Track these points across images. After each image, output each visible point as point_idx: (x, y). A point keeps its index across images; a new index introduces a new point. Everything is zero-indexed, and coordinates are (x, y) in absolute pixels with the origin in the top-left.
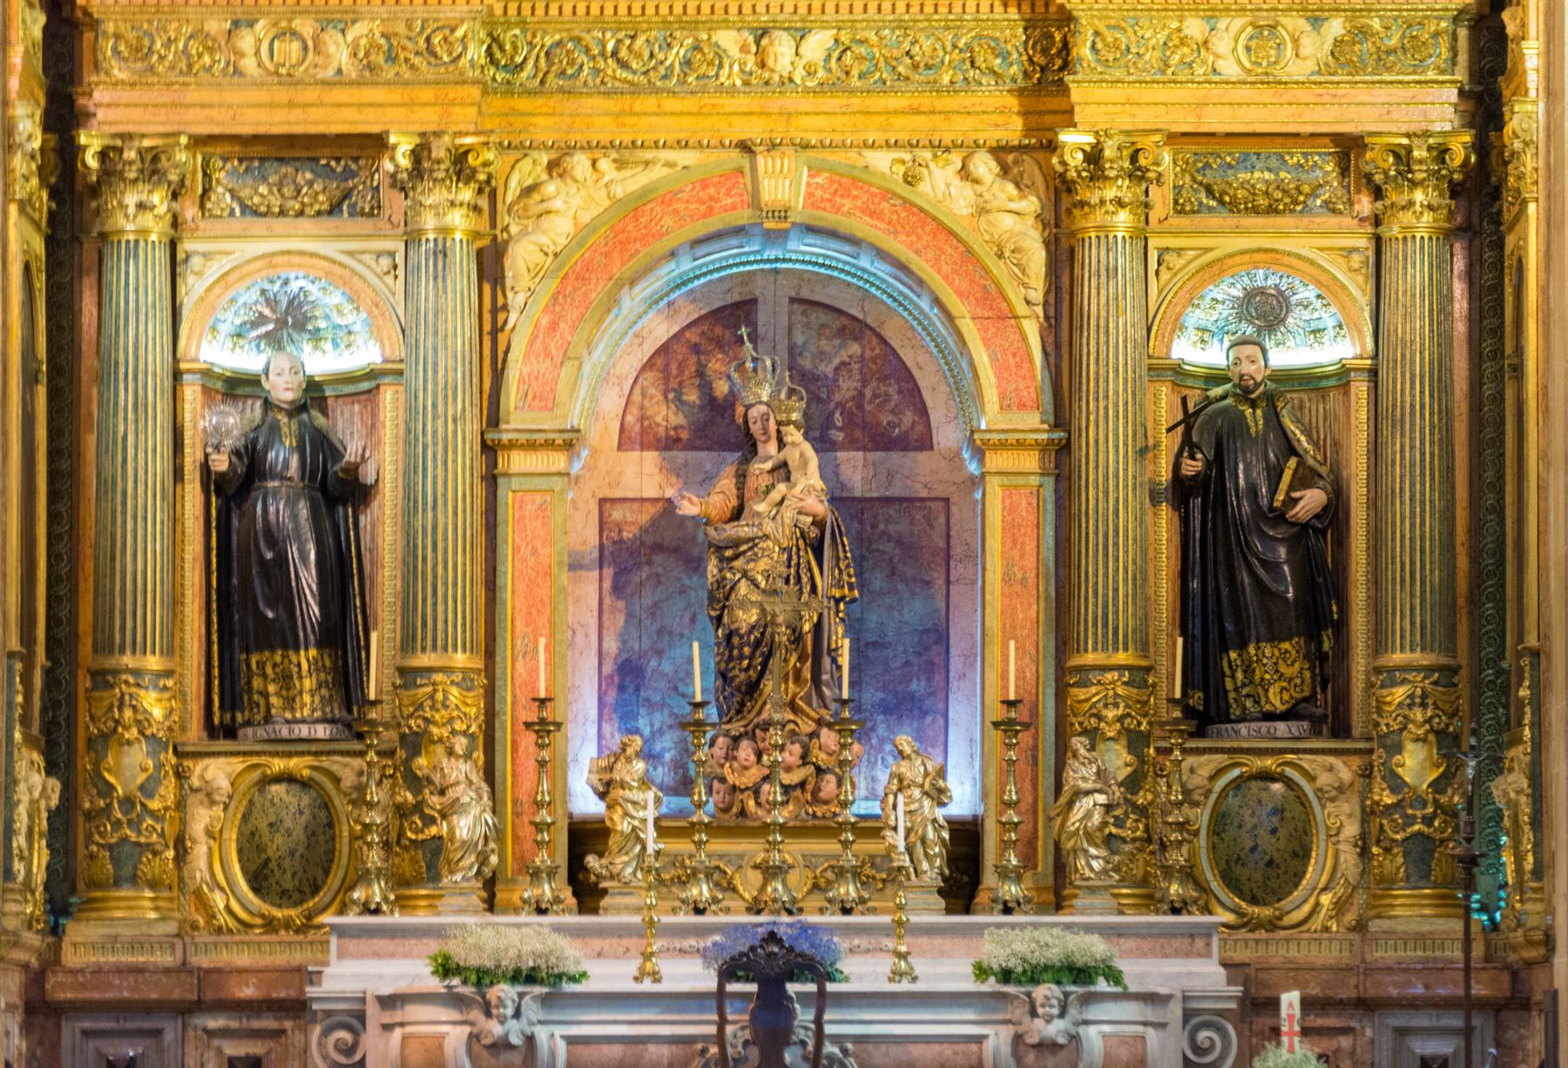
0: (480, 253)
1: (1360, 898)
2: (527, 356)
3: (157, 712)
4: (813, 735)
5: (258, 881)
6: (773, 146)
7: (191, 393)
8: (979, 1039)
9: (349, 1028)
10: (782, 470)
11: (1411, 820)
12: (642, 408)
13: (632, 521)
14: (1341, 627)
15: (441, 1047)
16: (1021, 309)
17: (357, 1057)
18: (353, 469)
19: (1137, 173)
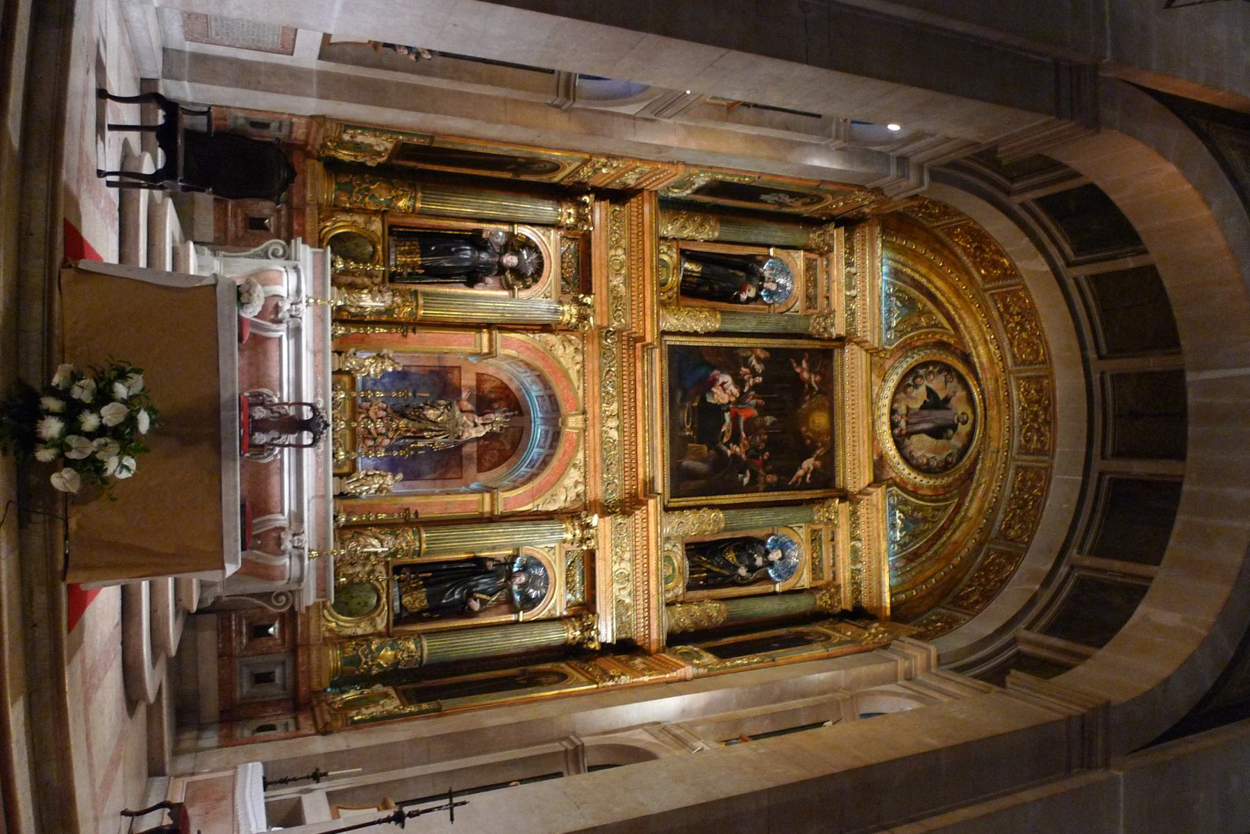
3: (401, 204)
4: (388, 438)
6: (585, 420)
8: (282, 512)
9: (283, 256)
10: (476, 425)
11: (366, 657)
14: (430, 619)
15: (277, 284)
16: (536, 503)
18: (482, 281)
19: (583, 541)
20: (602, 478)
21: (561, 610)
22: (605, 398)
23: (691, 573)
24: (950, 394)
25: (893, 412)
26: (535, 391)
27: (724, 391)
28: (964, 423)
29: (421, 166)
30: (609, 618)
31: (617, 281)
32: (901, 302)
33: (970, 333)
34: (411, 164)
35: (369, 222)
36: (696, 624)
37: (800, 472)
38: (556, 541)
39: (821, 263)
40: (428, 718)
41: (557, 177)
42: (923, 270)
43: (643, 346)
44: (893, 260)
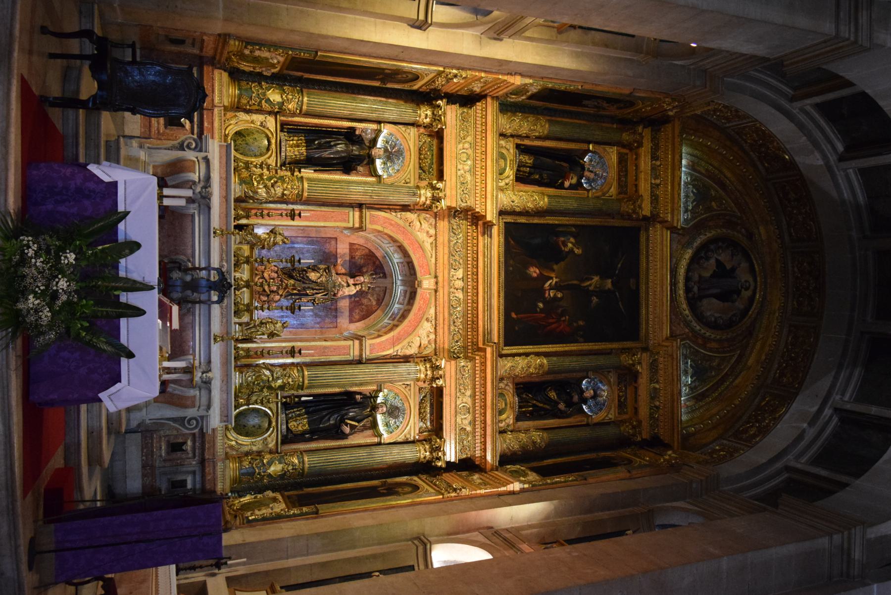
0: (409, 205)
1: (234, 453)
2: (384, 217)
5: (239, 134)
6: (437, 283)
7: (374, 126)
9: (196, 147)
10: (348, 286)
11: (259, 468)
12: (360, 249)
13: (329, 247)
16: (396, 348)
17: (186, 149)
18: (356, 169)
20: (449, 329)
21: (413, 434)
23: (520, 407)
25: (687, 279)
26: (397, 258)
28: (747, 289)
29: (306, 76)
30: (453, 442)
32: (696, 189)
34: (299, 74)
36: (523, 447)
38: (412, 380)
39: (631, 157)
40: (308, 519)
41: (416, 86)
43: (484, 224)
44: (691, 155)
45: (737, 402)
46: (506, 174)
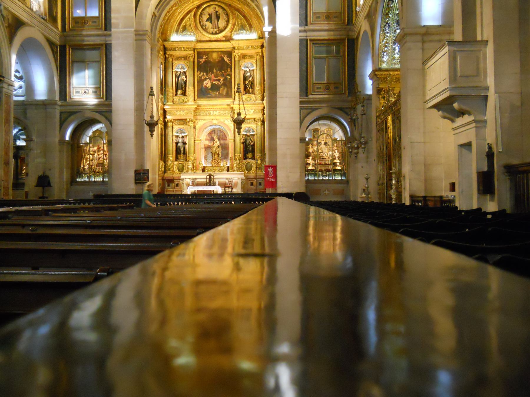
0: (194, 127)
5: (179, 170)
10: (216, 142)
13: (206, 146)
22: (210, 114)
23: (250, 93)
24: (208, 13)
25: (212, 34)
27: (208, 84)
31: (184, 113)
33: (191, 7)
35: (175, 165)
37: (228, 61)
41: (163, 127)
42: (175, 23)
45: (252, 14)
46: (183, 99)
